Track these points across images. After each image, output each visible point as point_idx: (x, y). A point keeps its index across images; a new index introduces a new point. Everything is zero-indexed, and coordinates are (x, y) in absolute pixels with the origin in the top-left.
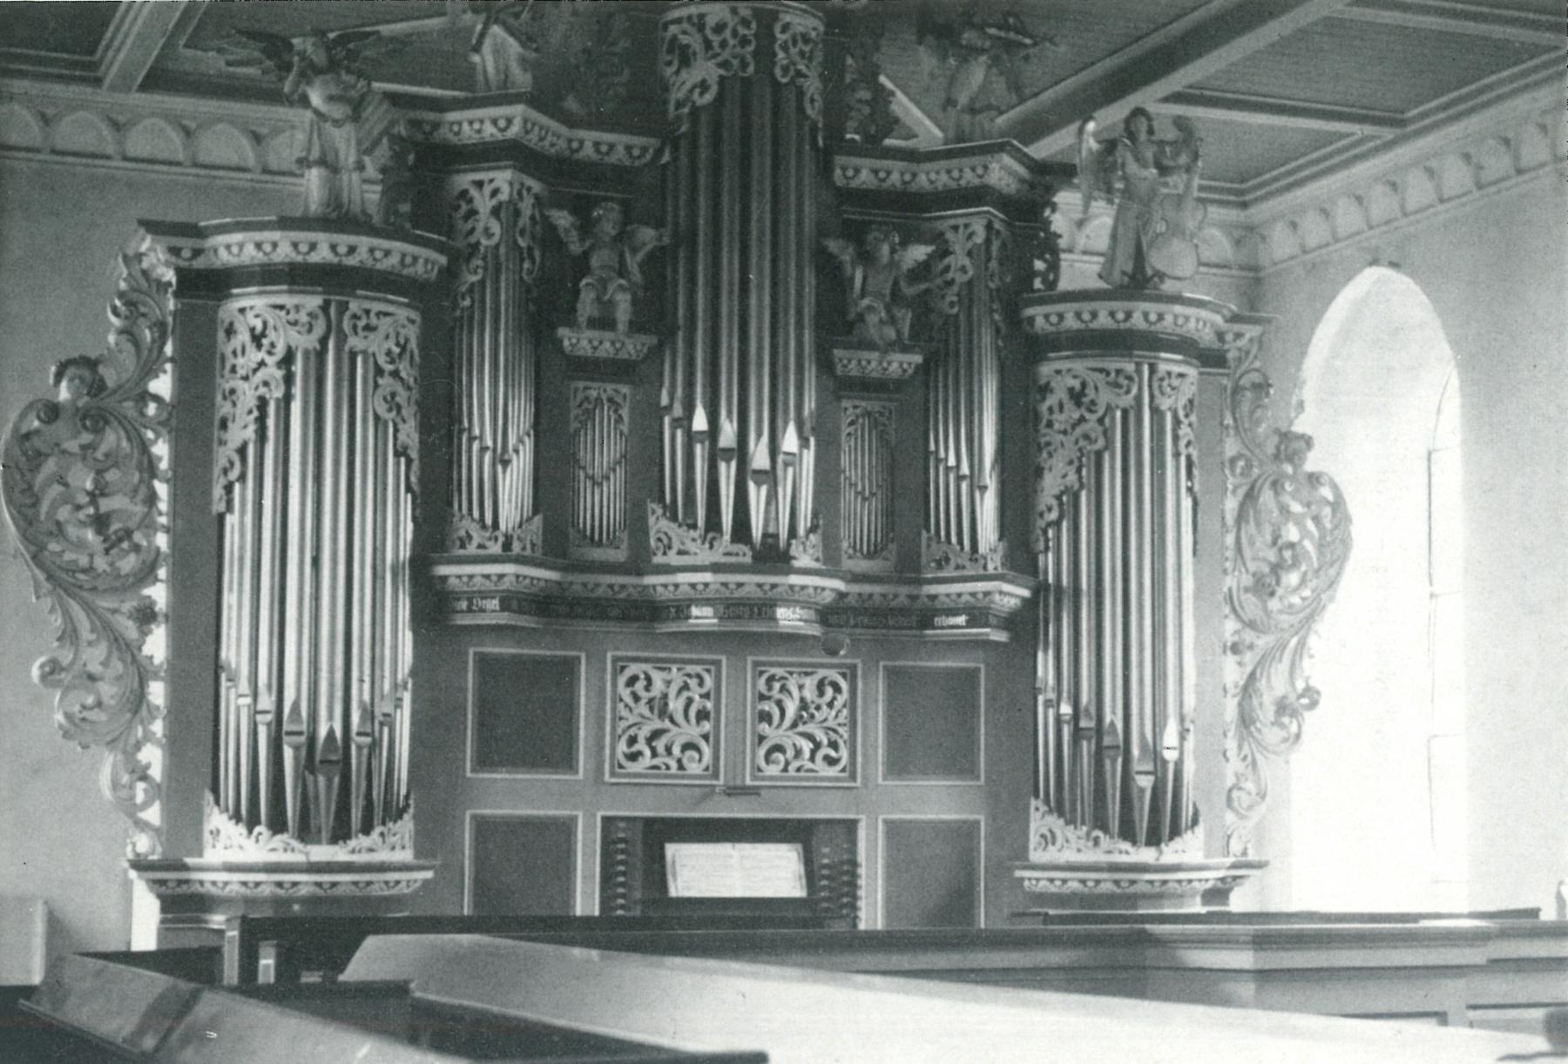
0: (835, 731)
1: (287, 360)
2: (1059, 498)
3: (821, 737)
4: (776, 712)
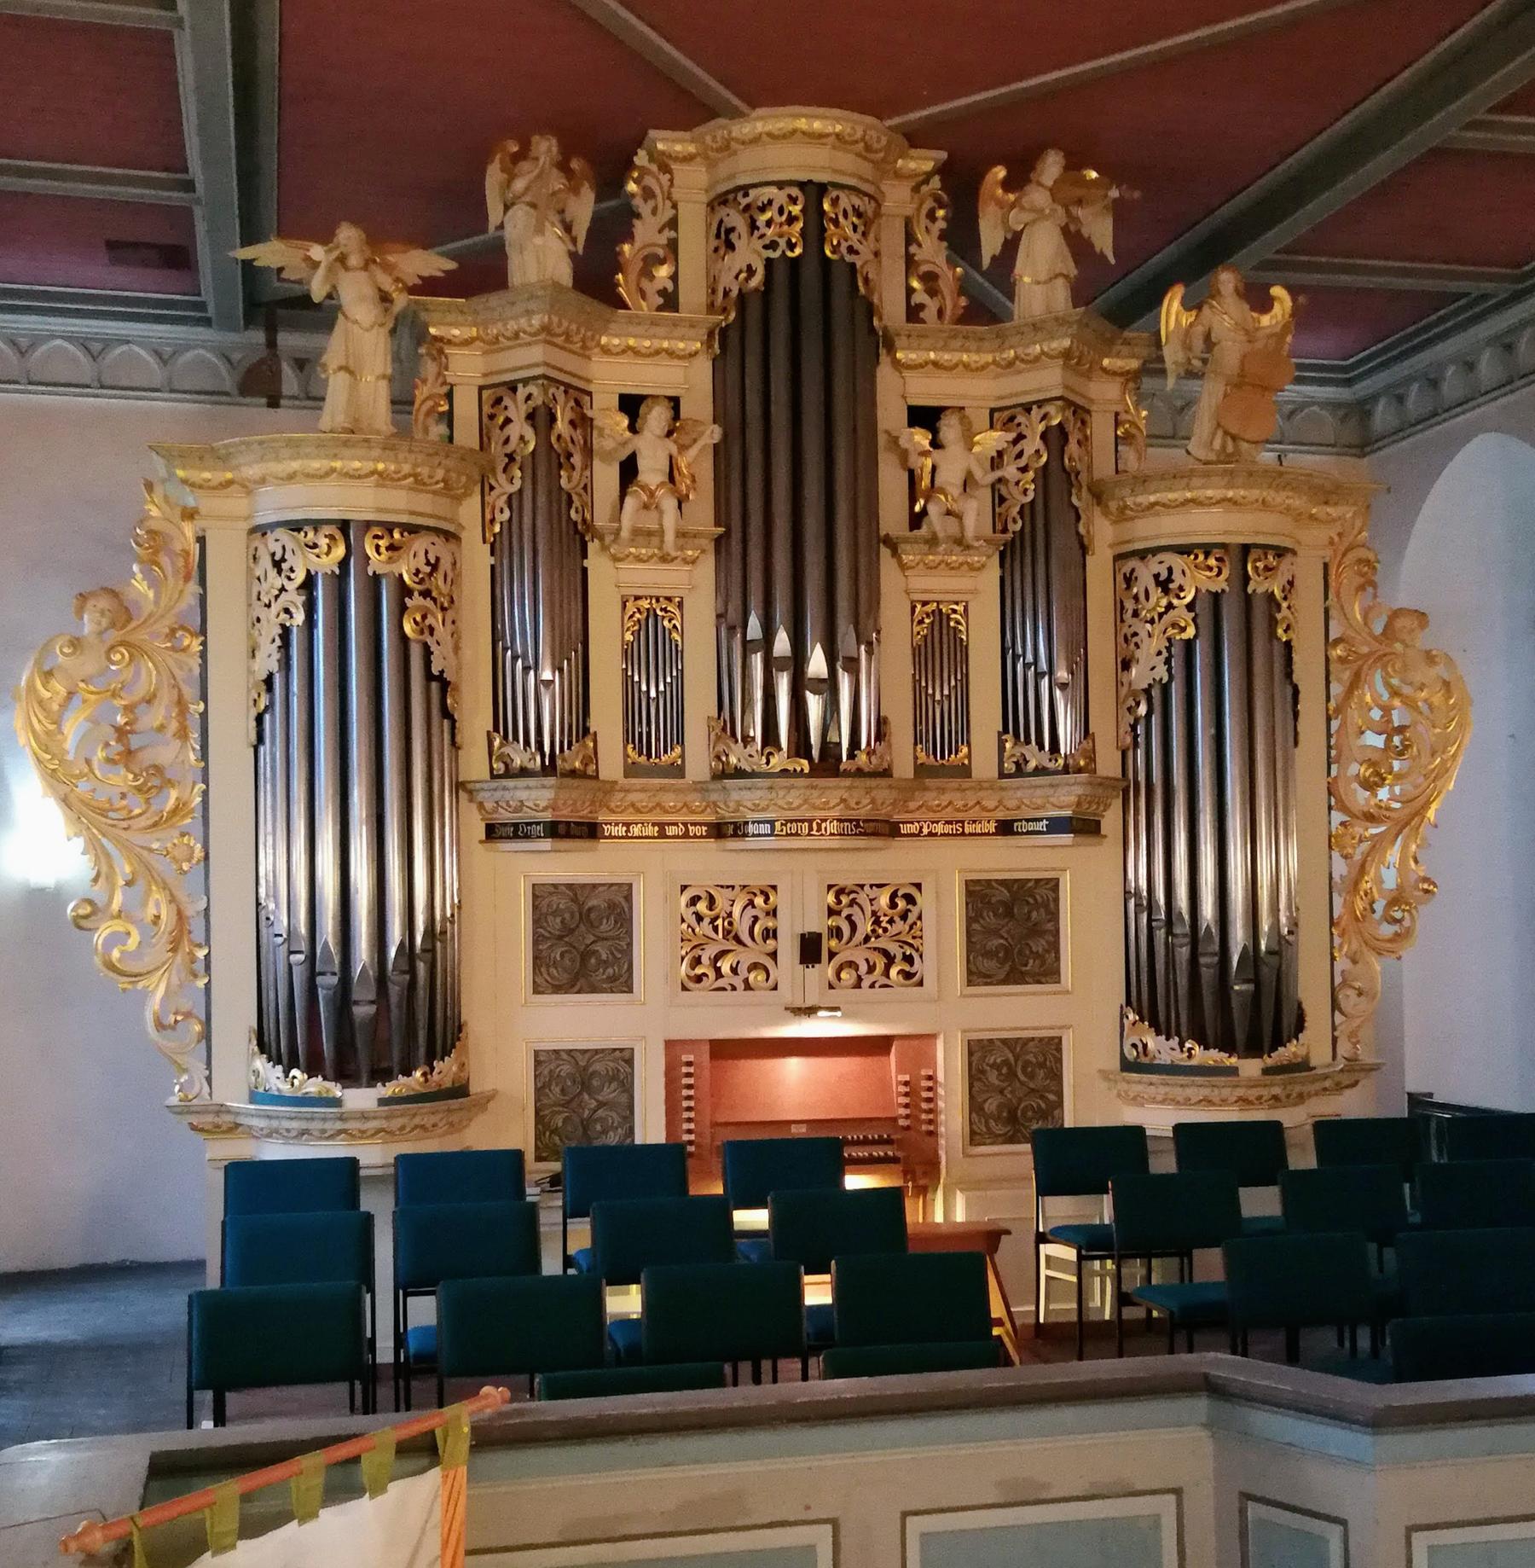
0: (911, 945)
2: (1147, 692)
3: (894, 948)
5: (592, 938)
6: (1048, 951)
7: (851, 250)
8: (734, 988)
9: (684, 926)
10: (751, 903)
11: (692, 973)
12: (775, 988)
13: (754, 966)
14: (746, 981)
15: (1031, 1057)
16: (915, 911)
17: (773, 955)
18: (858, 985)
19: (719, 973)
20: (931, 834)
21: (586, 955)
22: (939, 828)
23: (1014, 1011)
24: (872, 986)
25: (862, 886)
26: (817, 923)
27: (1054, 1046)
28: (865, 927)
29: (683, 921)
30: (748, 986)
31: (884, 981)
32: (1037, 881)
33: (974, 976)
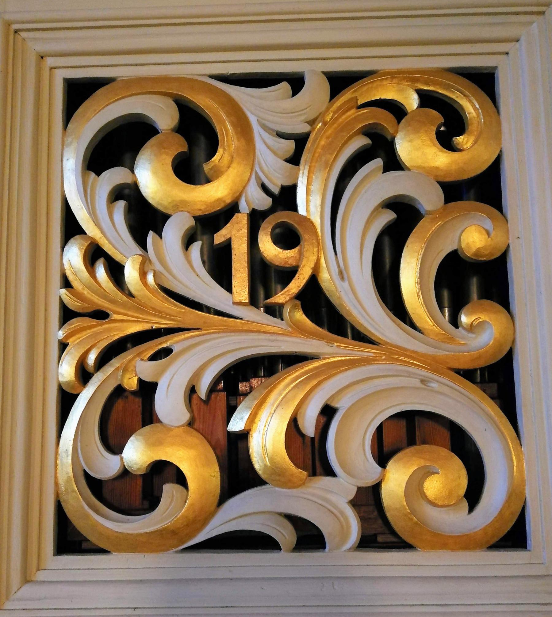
9: (74, 256)
11: (107, 466)
12: (514, 536)
14: (369, 500)
19: (237, 472)
29: (71, 228)
30: (380, 531)
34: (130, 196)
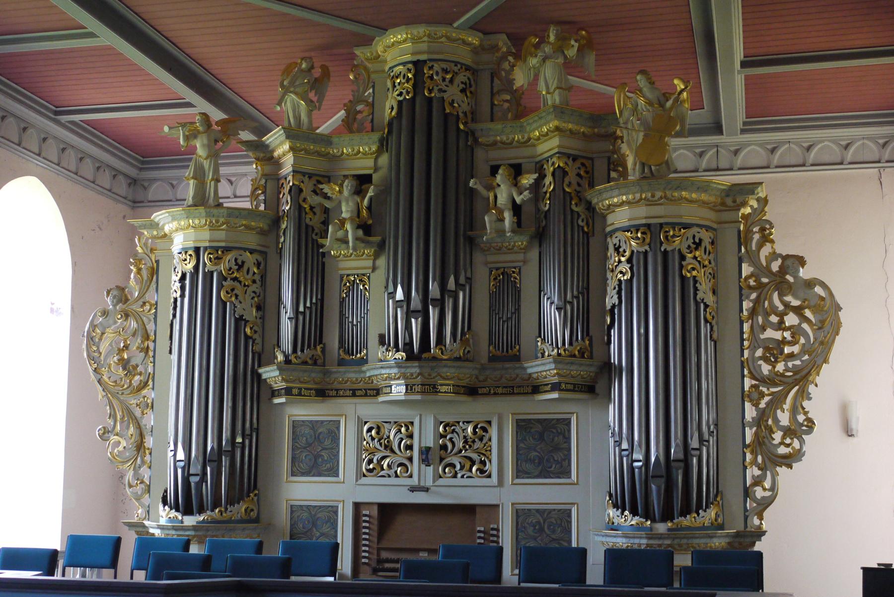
1: (184, 276)
3: (475, 456)
4: (450, 446)
5: (320, 448)
6: (564, 460)
7: (440, 90)
8: (389, 476)
9: (365, 443)
10: (400, 431)
12: (411, 476)
13: (400, 465)
14: (396, 472)
15: (553, 520)
16: (487, 436)
17: (410, 459)
18: (455, 476)
19: (382, 469)
20: (495, 394)
21: (316, 457)
22: (500, 390)
23: (541, 493)
24: (462, 477)
25: (458, 422)
26: (429, 441)
27: (566, 515)
28: (460, 444)
30: (397, 476)
31: (469, 474)
32: (558, 420)
33: (519, 473)
34: (371, 436)
